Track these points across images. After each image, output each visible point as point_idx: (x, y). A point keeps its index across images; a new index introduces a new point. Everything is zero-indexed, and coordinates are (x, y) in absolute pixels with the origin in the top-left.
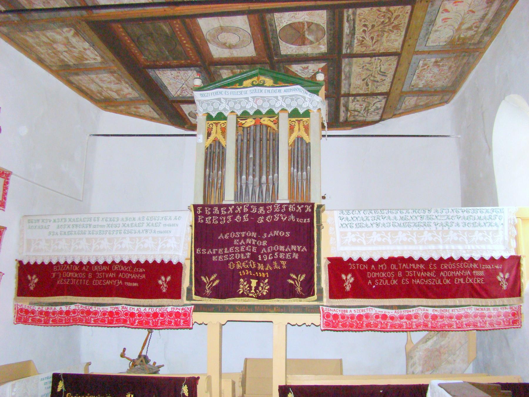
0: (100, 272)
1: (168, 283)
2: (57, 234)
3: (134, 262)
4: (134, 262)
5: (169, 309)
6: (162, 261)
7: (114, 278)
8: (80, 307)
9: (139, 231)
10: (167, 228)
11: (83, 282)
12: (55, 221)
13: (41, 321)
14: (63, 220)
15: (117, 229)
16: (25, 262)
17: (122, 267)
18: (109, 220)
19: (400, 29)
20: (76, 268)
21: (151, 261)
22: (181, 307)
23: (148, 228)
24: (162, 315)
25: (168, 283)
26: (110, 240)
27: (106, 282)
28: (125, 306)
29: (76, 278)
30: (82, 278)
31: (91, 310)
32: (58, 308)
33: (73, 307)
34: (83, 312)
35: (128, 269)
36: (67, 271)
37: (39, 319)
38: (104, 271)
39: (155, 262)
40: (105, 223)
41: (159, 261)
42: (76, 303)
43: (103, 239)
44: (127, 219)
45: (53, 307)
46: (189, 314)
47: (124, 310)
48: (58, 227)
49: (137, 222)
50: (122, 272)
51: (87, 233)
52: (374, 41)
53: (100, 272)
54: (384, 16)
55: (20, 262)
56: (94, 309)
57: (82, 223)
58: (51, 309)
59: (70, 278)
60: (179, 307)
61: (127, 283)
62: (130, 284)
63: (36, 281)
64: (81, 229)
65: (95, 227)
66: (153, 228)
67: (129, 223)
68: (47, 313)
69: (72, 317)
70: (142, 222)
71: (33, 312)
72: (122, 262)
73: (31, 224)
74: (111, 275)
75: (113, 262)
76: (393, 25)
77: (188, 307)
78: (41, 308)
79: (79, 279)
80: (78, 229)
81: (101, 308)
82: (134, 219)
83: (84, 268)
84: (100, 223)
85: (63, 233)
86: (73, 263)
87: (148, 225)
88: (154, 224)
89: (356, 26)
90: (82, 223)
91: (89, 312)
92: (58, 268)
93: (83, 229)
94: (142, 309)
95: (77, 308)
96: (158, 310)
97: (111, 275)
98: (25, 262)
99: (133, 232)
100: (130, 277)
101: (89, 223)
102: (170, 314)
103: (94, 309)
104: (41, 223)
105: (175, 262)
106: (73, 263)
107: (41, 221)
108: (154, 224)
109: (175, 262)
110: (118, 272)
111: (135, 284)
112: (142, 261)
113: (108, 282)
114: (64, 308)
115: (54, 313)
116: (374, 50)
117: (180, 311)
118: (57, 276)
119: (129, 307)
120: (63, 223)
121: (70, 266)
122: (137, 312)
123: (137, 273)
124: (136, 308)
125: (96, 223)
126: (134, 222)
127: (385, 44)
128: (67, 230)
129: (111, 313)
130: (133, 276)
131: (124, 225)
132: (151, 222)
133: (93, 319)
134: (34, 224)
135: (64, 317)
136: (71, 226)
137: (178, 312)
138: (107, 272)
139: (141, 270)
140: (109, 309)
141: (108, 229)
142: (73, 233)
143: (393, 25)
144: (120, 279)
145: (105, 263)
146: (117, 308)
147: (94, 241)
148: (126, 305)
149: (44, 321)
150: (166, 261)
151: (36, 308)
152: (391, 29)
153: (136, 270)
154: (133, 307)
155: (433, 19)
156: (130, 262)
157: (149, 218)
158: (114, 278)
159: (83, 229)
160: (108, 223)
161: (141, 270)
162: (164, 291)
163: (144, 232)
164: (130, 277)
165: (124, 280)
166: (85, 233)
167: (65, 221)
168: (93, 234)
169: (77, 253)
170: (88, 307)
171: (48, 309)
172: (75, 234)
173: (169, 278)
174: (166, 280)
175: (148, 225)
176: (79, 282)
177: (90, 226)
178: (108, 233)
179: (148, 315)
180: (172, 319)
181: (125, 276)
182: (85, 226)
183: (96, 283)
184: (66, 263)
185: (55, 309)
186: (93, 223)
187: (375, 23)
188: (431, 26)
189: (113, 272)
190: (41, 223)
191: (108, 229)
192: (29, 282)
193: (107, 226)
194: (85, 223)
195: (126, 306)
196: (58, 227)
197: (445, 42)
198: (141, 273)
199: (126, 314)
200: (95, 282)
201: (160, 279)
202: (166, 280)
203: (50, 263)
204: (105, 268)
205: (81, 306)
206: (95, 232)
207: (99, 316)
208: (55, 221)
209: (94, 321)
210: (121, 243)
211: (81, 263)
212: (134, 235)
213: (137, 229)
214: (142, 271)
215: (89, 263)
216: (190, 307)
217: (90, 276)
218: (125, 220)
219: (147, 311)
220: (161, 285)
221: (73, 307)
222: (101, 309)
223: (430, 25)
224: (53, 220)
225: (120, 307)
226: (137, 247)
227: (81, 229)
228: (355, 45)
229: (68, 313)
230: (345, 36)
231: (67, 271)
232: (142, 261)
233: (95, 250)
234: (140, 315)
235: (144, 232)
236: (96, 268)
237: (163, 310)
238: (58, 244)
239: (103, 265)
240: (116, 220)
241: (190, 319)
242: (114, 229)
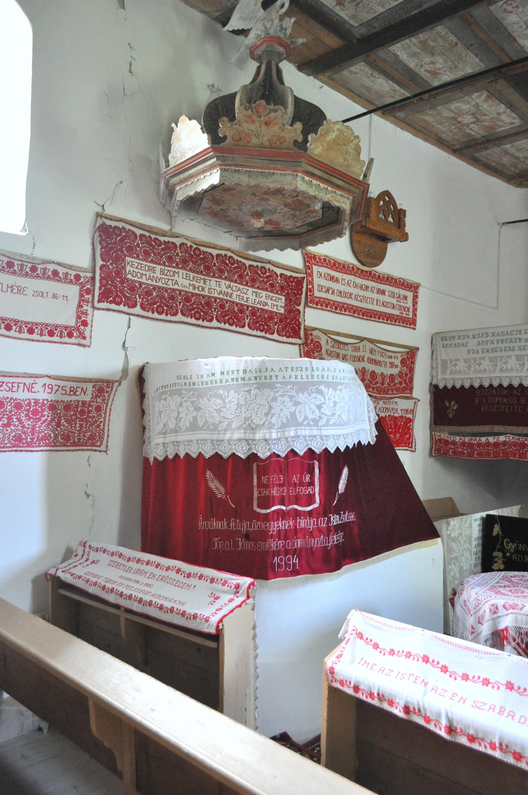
2: (478, 352)
11: (514, 409)
12: (474, 337)
14: (485, 335)
16: (441, 386)
20: (505, 392)
29: (504, 404)
30: (513, 404)
51: (517, 348)
55: (436, 387)
57: (509, 337)
64: (508, 345)
73: (445, 343)
80: (504, 344)
85: (485, 350)
86: (501, 386)
90: (509, 337)
92: (481, 392)
93: (511, 345)
98: (441, 386)
104: (456, 341)
107: (457, 337)
120: (484, 339)
128: (490, 346)
134: (449, 342)
136: (495, 342)
142: (498, 350)
159: (511, 345)
166: (513, 350)
167: (487, 337)
169: (505, 374)
172: (501, 350)
177: (520, 340)
182: (513, 340)
184: (491, 386)
190: (456, 341)
192: (447, 408)
194: (513, 337)
196: (479, 344)
203: (472, 387)
208: (474, 337)
211: (511, 386)
224: (471, 336)
227: (508, 345)
238: (480, 364)
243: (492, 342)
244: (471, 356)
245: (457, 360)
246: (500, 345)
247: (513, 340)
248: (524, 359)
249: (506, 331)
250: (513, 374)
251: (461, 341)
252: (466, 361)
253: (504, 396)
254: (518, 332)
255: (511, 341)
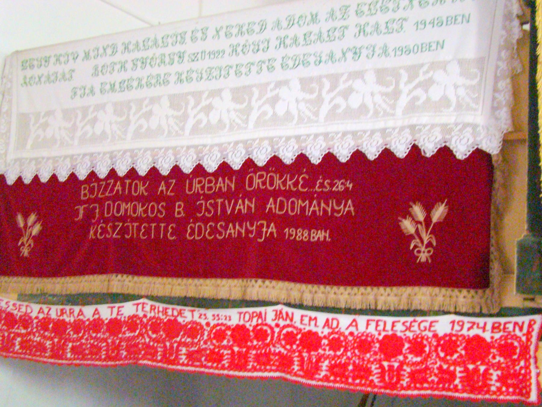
0: (207, 197)
1: (438, 230)
2: (92, 91)
3: (316, 158)
4: (316, 158)
5: (443, 325)
6: (415, 150)
7: (250, 217)
8: (148, 308)
9: (331, 56)
10: (432, 34)
11: (158, 228)
12: (87, 56)
13: (45, 349)
14: (109, 51)
15: (261, 56)
17: (276, 177)
18: (235, 31)
21: (372, 153)
22: (490, 321)
23: (362, 41)
24: (417, 346)
25: (438, 230)
26: (239, 94)
27: (226, 228)
28: (285, 309)
30: (156, 220)
31: (180, 319)
32: (88, 312)
33: (128, 309)
34: (155, 325)
35: (296, 184)
36: (116, 198)
37: (39, 343)
38: (219, 194)
39: (387, 154)
40: (224, 44)
41: (401, 151)
42: (140, 297)
43: (217, 93)
44: (291, 23)
45: (77, 309)
46: (525, 349)
47: (282, 323)
48: (96, 73)
49: (325, 26)
50: (276, 194)
51: (173, 79)
53: (207, 197)
56: (188, 316)
57: (158, 52)
58: (72, 314)
59: (124, 219)
60: (481, 321)
61: (293, 231)
62: (301, 235)
63: (36, 230)
64: (155, 71)
65: (195, 57)
66: (379, 40)
67: (297, 31)
68: (60, 327)
69: (129, 339)
70: (338, 24)
71: (26, 321)
72: (275, 162)
73: (29, 73)
74: (243, 206)
75: (249, 164)
77: (519, 319)
78: (46, 311)
79: (150, 220)
80: (148, 70)
81: (210, 313)
82: (314, 18)
83: (162, 187)
84: (210, 45)
85: (108, 87)
86: (132, 173)
87: (362, 31)
88: (383, 28)
90: (158, 52)
91: (172, 328)
92: (91, 191)
93: (162, 70)
94: (344, 320)
95: (141, 314)
96: (398, 326)
97: (243, 206)
99: (312, 59)
100: (303, 209)
101: (179, 48)
102: (448, 344)
103: (188, 316)
104: (52, 68)
105: (461, 151)
106: (132, 173)
107: (53, 60)
108: (383, 28)
109: (461, 151)
110: (262, 196)
111: (320, 235)
112: (343, 155)
113: (233, 230)
114: (106, 312)
115: (78, 326)
117: (487, 336)
118: (89, 214)
119: (298, 313)
120: (107, 60)
121: (123, 185)
122: (327, 331)
123: (326, 197)
124: (322, 317)
125: (199, 46)
126: (314, 28)
128: (117, 77)
129: (240, 333)
130: (314, 208)
131: (282, 42)
132: (372, 20)
133: (184, 350)
134: (37, 72)
135: (105, 340)
136: (129, 66)
137: (477, 338)
138: (230, 195)
139: (339, 186)
140: (233, 317)
141: (234, 60)
142: (135, 84)
144: (270, 217)
145: (224, 169)
146: (260, 315)
147: (192, 102)
148: (289, 305)
149: (52, 350)
150: (429, 149)
151: (35, 310)
153: (322, 185)
154: (313, 314)
156: (302, 159)
157: (365, 9)
158: (250, 217)
159: (162, 70)
160: (234, 41)
161: (339, 186)
162: (424, 256)
163: (349, 55)
164: (303, 209)
165: (285, 221)
166: (166, 82)
167: (114, 53)
168: (189, 79)
170: (172, 310)
171: (62, 312)
172: (140, 86)
173: (439, 212)
174: (428, 220)
175: (362, 31)
176: (148, 231)
178: (232, 72)
179: (364, 344)
180: (455, 363)
181: (287, 207)
182: (167, 60)
183: (196, 232)
185: (81, 313)
186: (190, 48)
189: (248, 195)
190: (52, 68)
191: (234, 60)
193: (228, 50)
194: (168, 51)
195: (290, 310)
196: (96, 73)
198: (340, 197)
199: (290, 338)
200: (193, 230)
201: (407, 214)
202: (428, 220)
204: (222, 184)
205: (153, 308)
206: (194, 76)
207: (204, 342)
209: (190, 355)
210: (274, 100)
212: (313, 71)
213: (324, 48)
214: (341, 188)
215: (176, 170)
216: (526, 319)
217: (179, 210)
218: (284, 24)
219: (362, 328)
220: (411, 237)
221: (128, 309)
222: (208, 317)
224: (82, 55)
225: (270, 312)
226: (325, 109)
227: (155, 71)
229: (115, 326)
231: (116, 198)
232: (343, 155)
233: (195, 130)
234: (335, 344)
235: (349, 55)
236: (197, 186)
237: (419, 326)
239: (216, 174)
240: (257, 28)
241: (527, 367)
242: (250, 57)
243: (123, 67)
244: (79, 102)
245: (49, 113)
246: (140, 73)
247: (167, 60)
248: (187, 104)
249: (152, 38)
250: (160, 142)
251: (60, 69)
252: (67, 114)
253: (140, 198)
254: (179, 38)
255: (163, 62)
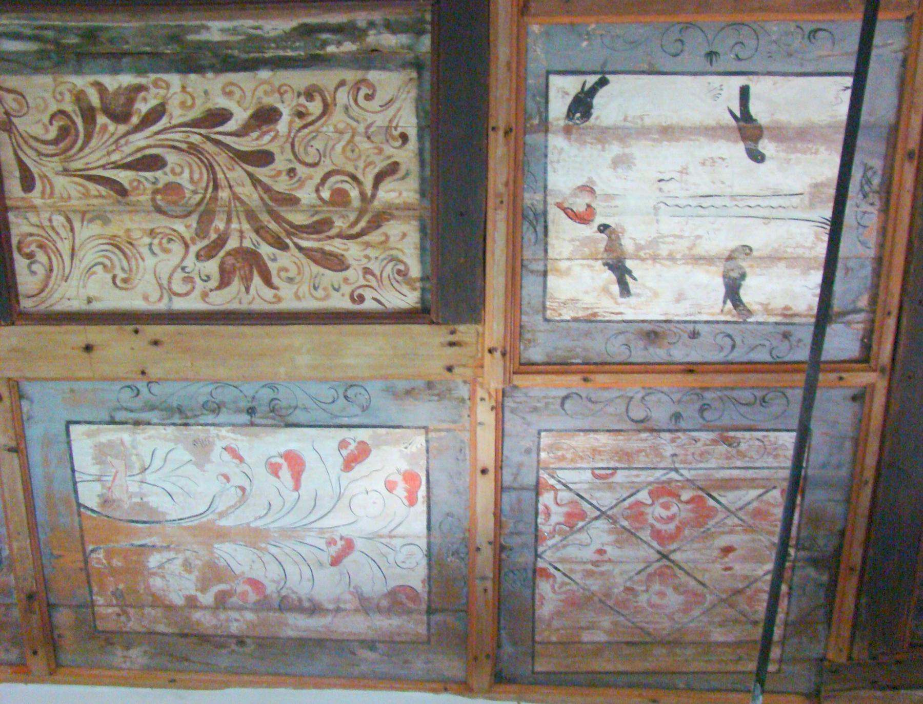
19: (224, 282)
52: (124, 177)
54: (340, 198)
76: (265, 250)
89: (264, 74)
116: (28, 182)
127: (85, 231)
143: (265, 250)
152: (232, 243)
155: (299, 416)
187: (281, 162)
188: (245, 418)
197: (106, 501)
223: (251, 411)
228: (80, 82)
230: (166, 21)
